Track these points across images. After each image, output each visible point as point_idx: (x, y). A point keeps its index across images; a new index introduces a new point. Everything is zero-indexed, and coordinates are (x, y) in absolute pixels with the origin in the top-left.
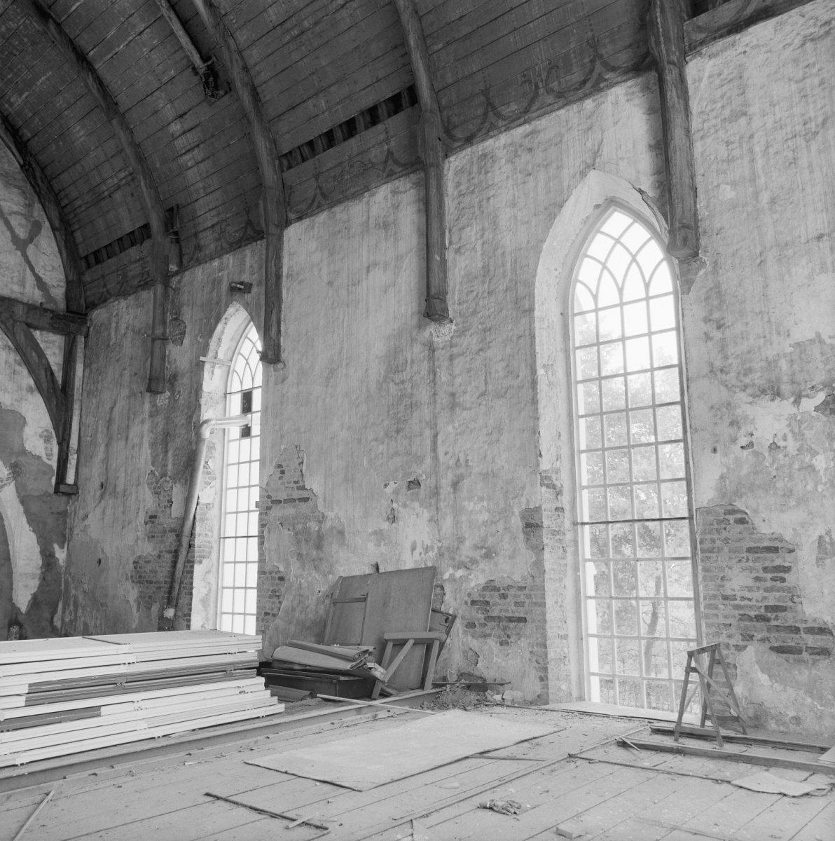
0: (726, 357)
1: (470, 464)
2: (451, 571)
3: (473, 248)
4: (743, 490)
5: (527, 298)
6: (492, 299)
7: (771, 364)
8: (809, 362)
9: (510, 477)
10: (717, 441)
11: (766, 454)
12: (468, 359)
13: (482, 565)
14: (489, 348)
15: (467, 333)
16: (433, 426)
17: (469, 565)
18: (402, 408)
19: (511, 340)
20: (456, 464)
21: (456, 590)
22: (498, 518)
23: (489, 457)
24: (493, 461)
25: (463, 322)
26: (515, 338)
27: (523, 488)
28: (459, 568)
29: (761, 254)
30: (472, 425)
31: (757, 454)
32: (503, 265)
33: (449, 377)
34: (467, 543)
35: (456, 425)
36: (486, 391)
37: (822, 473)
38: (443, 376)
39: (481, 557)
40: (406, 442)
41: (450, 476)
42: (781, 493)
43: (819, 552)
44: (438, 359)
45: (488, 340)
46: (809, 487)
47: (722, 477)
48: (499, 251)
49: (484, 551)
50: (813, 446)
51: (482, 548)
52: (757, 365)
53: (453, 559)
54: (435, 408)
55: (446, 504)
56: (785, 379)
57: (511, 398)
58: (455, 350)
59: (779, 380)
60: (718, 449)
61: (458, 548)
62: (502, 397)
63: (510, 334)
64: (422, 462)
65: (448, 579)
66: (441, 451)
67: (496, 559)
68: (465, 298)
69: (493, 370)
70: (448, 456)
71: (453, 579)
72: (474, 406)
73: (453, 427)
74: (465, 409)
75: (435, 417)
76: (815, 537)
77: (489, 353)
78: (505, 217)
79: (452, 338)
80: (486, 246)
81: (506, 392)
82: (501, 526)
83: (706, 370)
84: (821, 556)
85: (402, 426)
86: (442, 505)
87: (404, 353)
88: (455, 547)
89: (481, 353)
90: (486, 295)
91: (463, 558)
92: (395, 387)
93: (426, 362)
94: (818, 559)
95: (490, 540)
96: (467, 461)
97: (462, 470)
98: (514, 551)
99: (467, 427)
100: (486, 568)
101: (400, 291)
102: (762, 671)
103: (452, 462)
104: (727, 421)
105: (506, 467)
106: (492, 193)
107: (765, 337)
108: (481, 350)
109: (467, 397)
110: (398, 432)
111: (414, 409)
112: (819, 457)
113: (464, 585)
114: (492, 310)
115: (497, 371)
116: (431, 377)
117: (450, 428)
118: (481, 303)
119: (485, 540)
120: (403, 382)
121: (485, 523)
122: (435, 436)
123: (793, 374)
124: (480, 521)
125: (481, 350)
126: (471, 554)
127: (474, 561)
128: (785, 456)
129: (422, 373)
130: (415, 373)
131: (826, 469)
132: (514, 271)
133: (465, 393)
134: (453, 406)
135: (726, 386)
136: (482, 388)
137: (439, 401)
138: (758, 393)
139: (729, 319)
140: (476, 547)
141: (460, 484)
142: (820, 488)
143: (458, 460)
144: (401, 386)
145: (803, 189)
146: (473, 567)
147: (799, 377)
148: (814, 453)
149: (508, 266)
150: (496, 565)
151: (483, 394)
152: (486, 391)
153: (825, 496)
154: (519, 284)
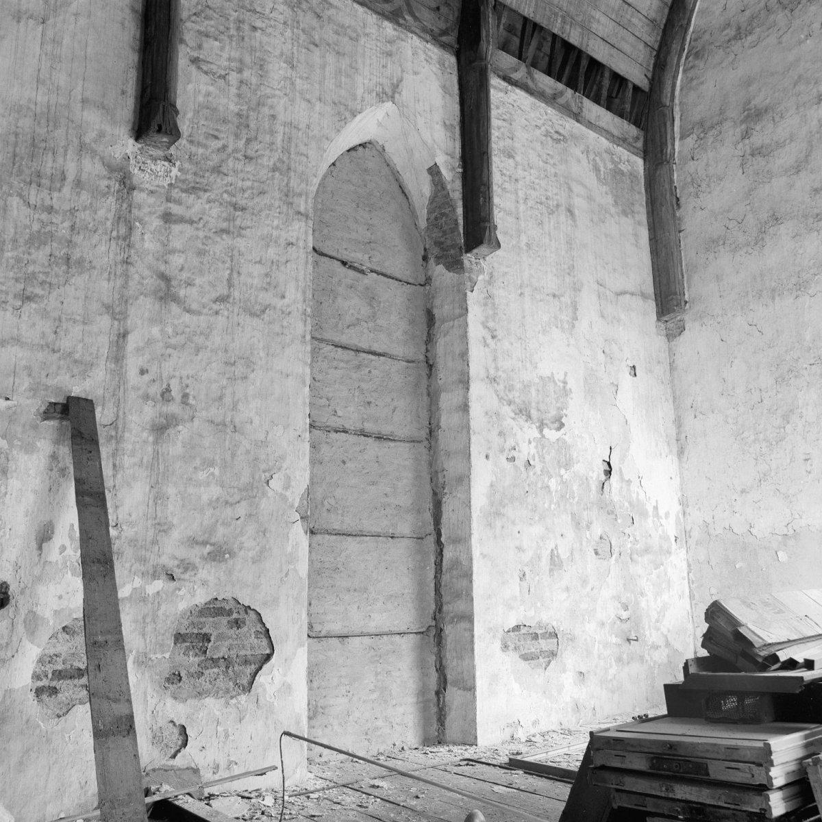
0: (497, 369)
1: (191, 401)
2: (138, 582)
3: (223, 77)
4: (506, 501)
5: (304, 197)
6: (249, 168)
7: (526, 387)
8: (548, 396)
9: (262, 437)
10: (490, 448)
11: (523, 469)
12: (201, 234)
13: (203, 574)
14: (240, 235)
15: (201, 193)
16: (117, 311)
17: (177, 573)
18: (41, 255)
19: (276, 242)
20: (162, 395)
22: (237, 498)
23: (228, 400)
24: (234, 407)
25: (195, 174)
26: (282, 242)
27: (282, 458)
28: (155, 576)
29: (521, 287)
30: (200, 340)
31: (516, 467)
32: (272, 132)
33: (158, 247)
34: (176, 534)
35: (170, 330)
36: (228, 296)
37: (554, 494)
38: (148, 243)
39: (203, 558)
40: (46, 326)
41: (150, 412)
42: (530, 507)
43: (551, 564)
44: (140, 207)
45: (238, 222)
46: (546, 505)
47: (492, 486)
48: (266, 111)
49: (208, 548)
50: (550, 469)
51: (204, 543)
52: (518, 386)
54: (125, 286)
55: (136, 460)
56: (533, 404)
57: (270, 323)
58: (176, 209)
59: (530, 403)
60: (491, 456)
61: (155, 542)
62: (258, 316)
63: (275, 233)
64: (84, 375)
66: (132, 364)
67: (231, 562)
68: (201, 139)
69: (244, 270)
70: (146, 377)
71: (140, 597)
72: (205, 311)
73: (162, 330)
74: (189, 311)
75: (125, 300)
76: (549, 551)
77: (241, 243)
78: (278, 70)
79: (170, 185)
80: (244, 87)
81: (263, 311)
82: (242, 510)
83: (483, 374)
84: (552, 567)
85: (38, 291)
86: (127, 461)
87: (60, 160)
88: (149, 539)
89: (224, 236)
90: (239, 155)
92: (26, 211)
93: (111, 200)
94: (551, 570)
95: (221, 533)
96: (185, 396)
97: (174, 408)
98: (261, 552)
99: (190, 339)
100: (211, 578)
101: (56, 42)
102: (516, 681)
103: (155, 390)
104: (495, 432)
105: (256, 420)
106: (258, 24)
107: (522, 362)
108: (223, 231)
109: (193, 292)
110: (27, 298)
111: (73, 270)
112: (553, 480)
113: (163, 607)
114: (249, 183)
115: (250, 275)
116: (123, 230)
117: (155, 331)
118: (231, 163)
119: (212, 530)
120: (50, 210)
121: (214, 504)
122: (124, 335)
123: (538, 403)
124: (205, 498)
125: (226, 231)
126: (182, 553)
127: (187, 566)
128: (534, 474)
129: (101, 213)
130: (85, 209)
131: (556, 491)
132: (286, 150)
133: (189, 284)
134: (166, 292)
135: (498, 396)
136: (222, 290)
137: (136, 276)
138: (518, 411)
139: (500, 334)
140: (193, 542)
141: (171, 431)
142: (553, 506)
143: (168, 390)
144: (44, 216)
145: (545, 250)
146: (186, 576)
147: (542, 407)
148: (550, 477)
149: (279, 138)
150: (230, 572)
151: (222, 299)
152: (228, 296)
153: (555, 514)
154: (292, 174)
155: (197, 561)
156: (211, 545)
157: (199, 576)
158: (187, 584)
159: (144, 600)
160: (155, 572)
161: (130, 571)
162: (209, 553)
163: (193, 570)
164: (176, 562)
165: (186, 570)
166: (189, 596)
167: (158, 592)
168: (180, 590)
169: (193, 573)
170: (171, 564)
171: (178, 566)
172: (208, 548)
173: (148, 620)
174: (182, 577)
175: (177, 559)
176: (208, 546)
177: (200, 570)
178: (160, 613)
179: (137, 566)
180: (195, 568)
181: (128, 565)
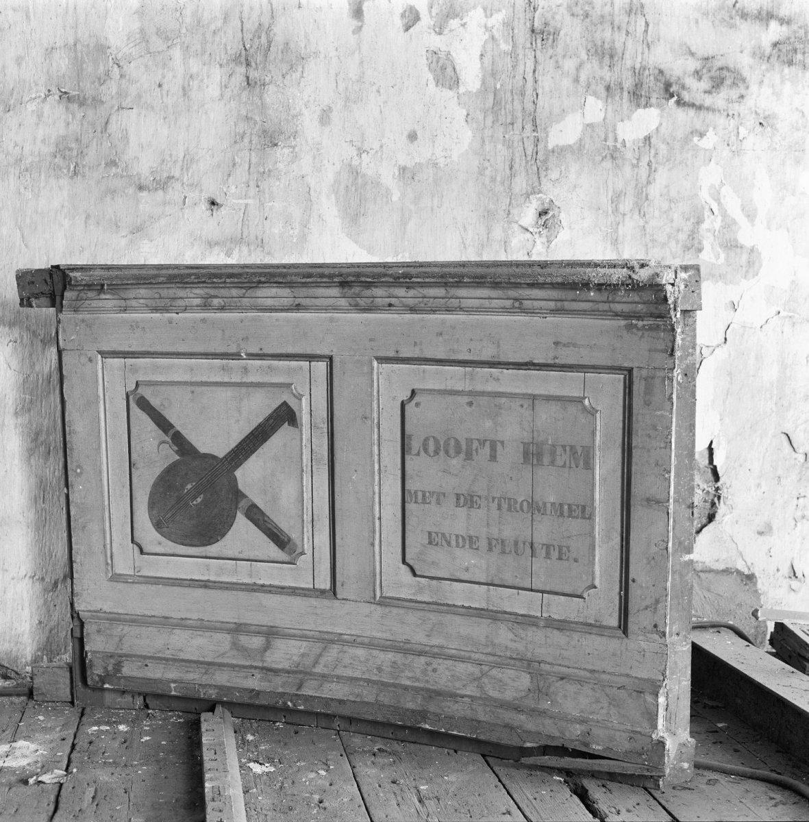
2: (595, 109)
13: (760, 96)
17: (696, 89)
21: (617, 198)
28: (638, 97)
39: (760, 55)
49: (775, 31)
53: (607, 54)
65: (577, 150)
91: (663, 57)
113: (662, 177)
126: (707, 40)
146: (719, 100)
155: (744, 62)
156: (783, 21)
157: (750, 102)
158: (721, 121)
159: (614, 155)
160: (638, 85)
161: (577, 80)
162: (775, 45)
163: (734, 84)
164: (692, 65)
165: (718, 83)
166: (726, 153)
167: (648, 139)
168: (702, 135)
169: (734, 94)
170: (679, 67)
171: (698, 74)
172: (775, 31)
173: (627, 205)
174: (708, 101)
175: (692, 54)
176: (774, 24)
177: (754, 88)
178: (654, 191)
179: (592, 68)
180: (739, 80)
181: (569, 65)
